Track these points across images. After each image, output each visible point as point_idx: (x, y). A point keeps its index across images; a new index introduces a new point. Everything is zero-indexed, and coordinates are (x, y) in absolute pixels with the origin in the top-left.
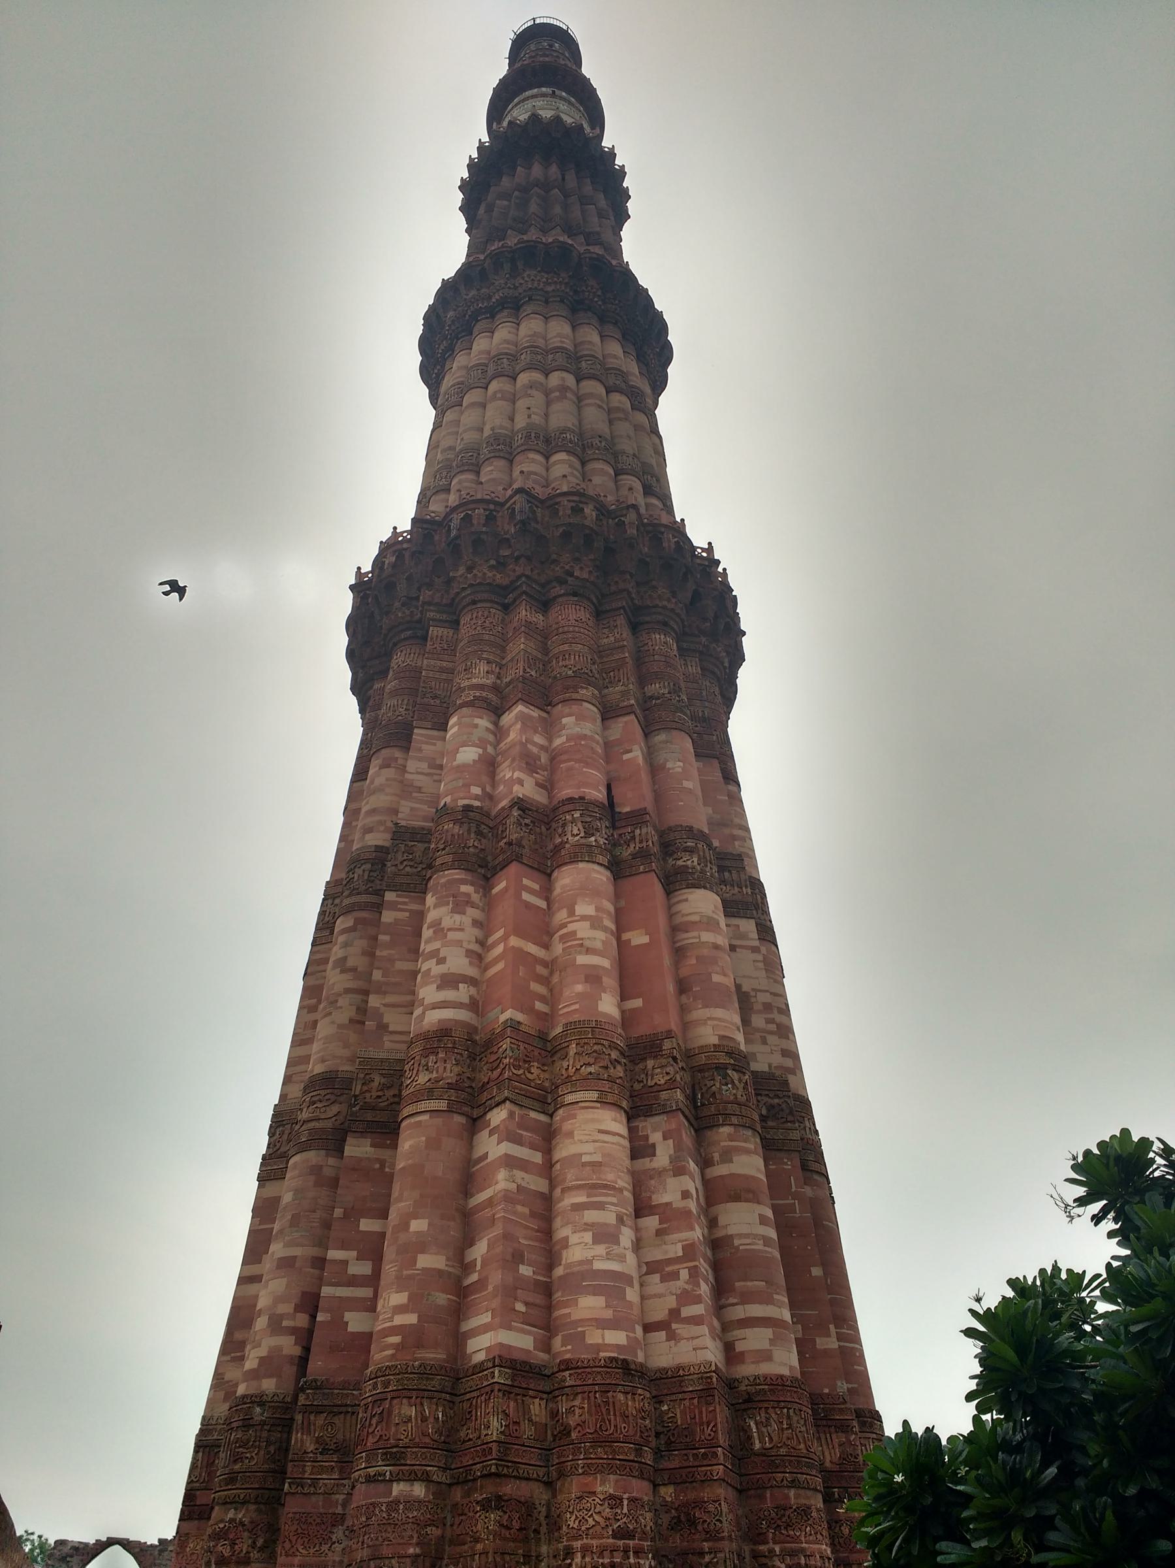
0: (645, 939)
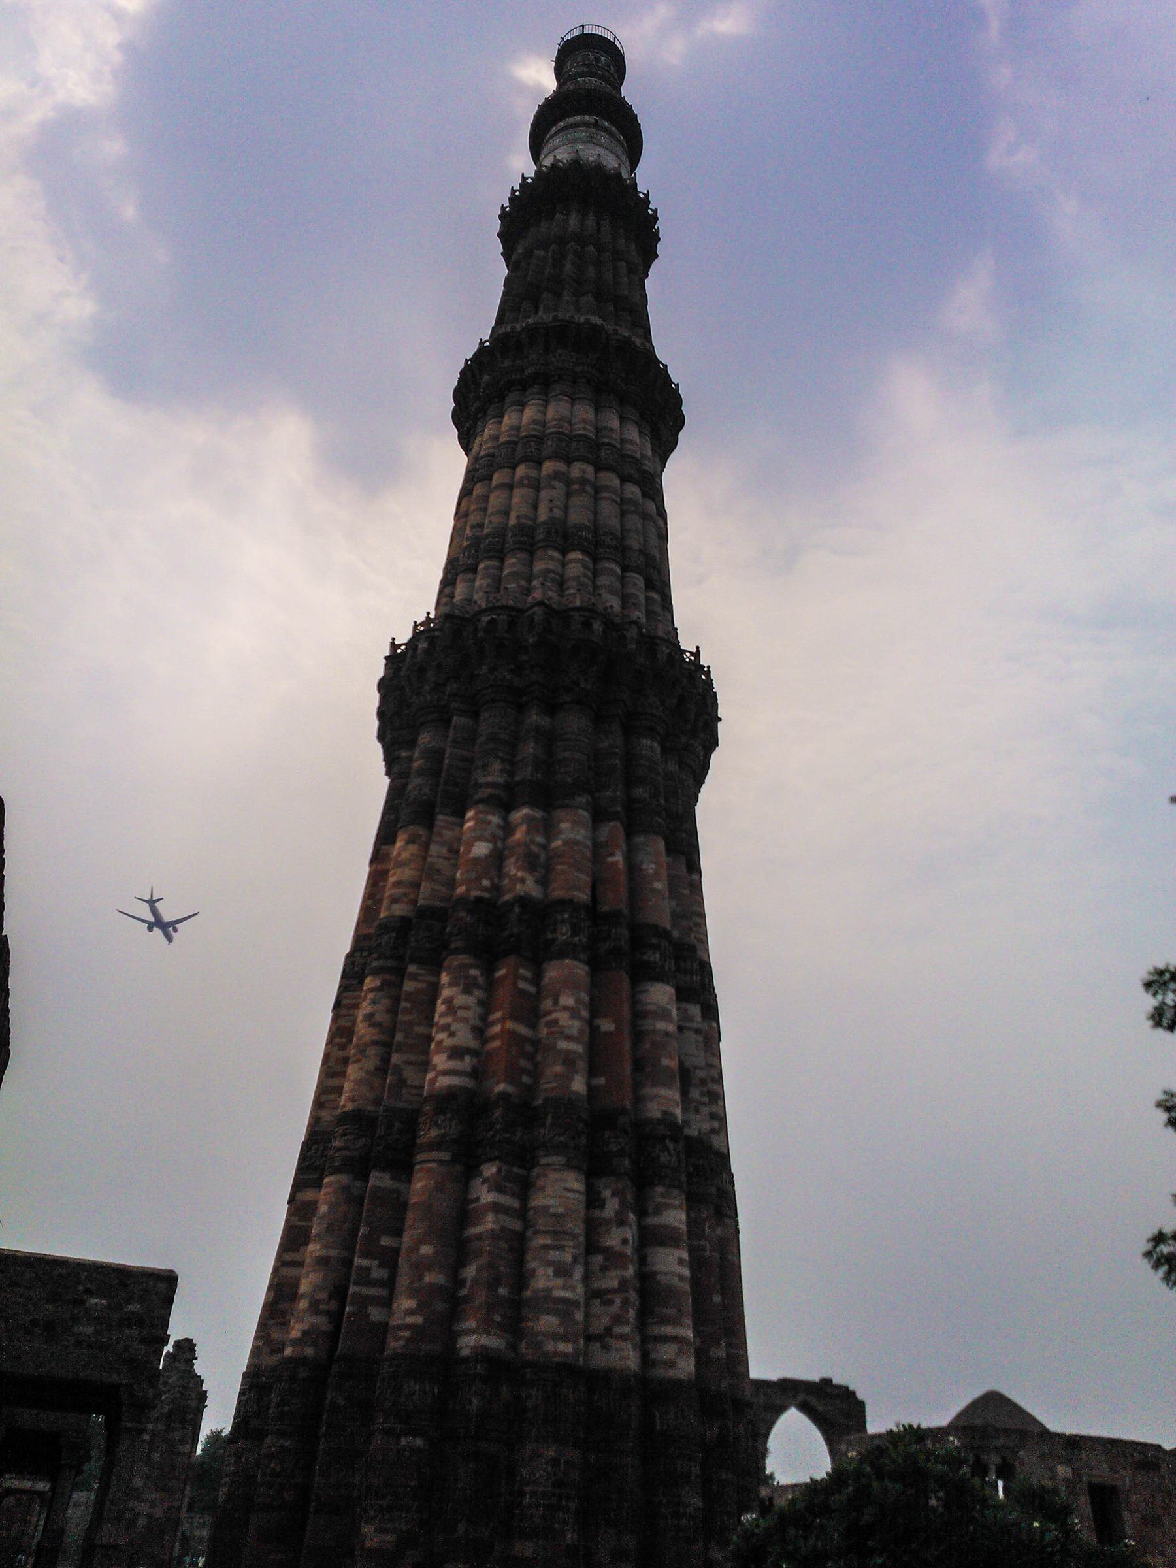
0: (612, 1027)
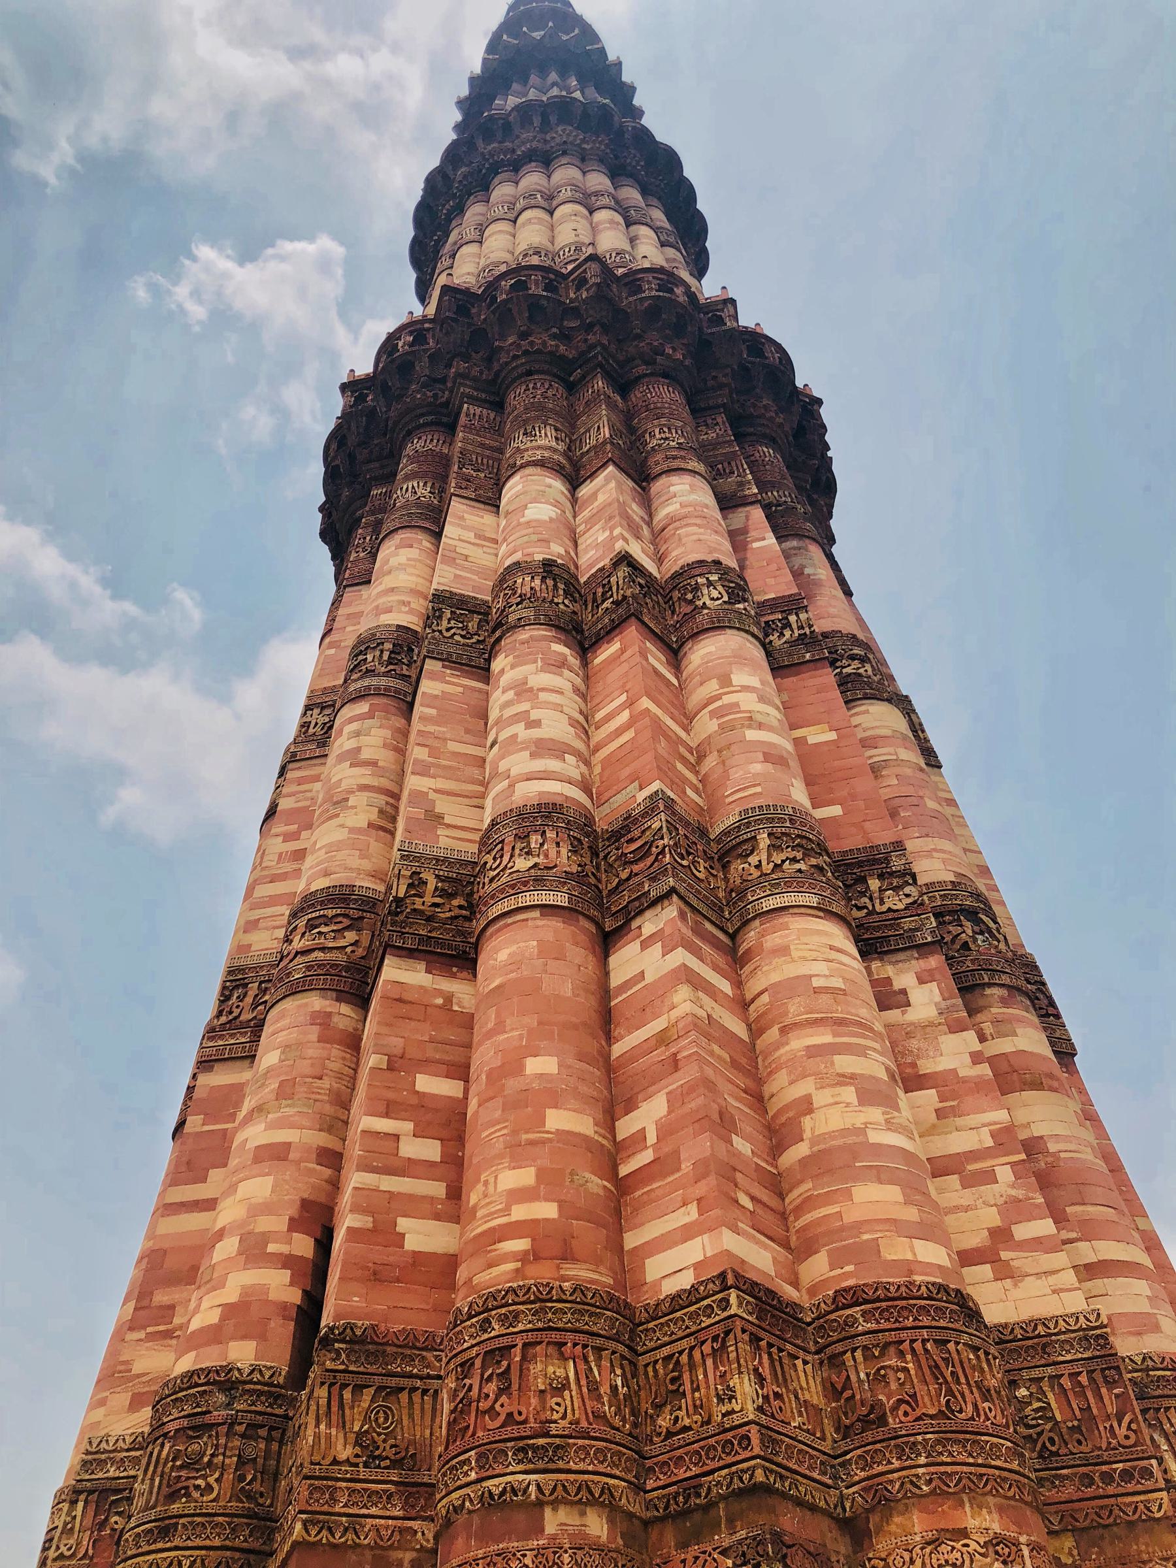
0: (833, 736)
